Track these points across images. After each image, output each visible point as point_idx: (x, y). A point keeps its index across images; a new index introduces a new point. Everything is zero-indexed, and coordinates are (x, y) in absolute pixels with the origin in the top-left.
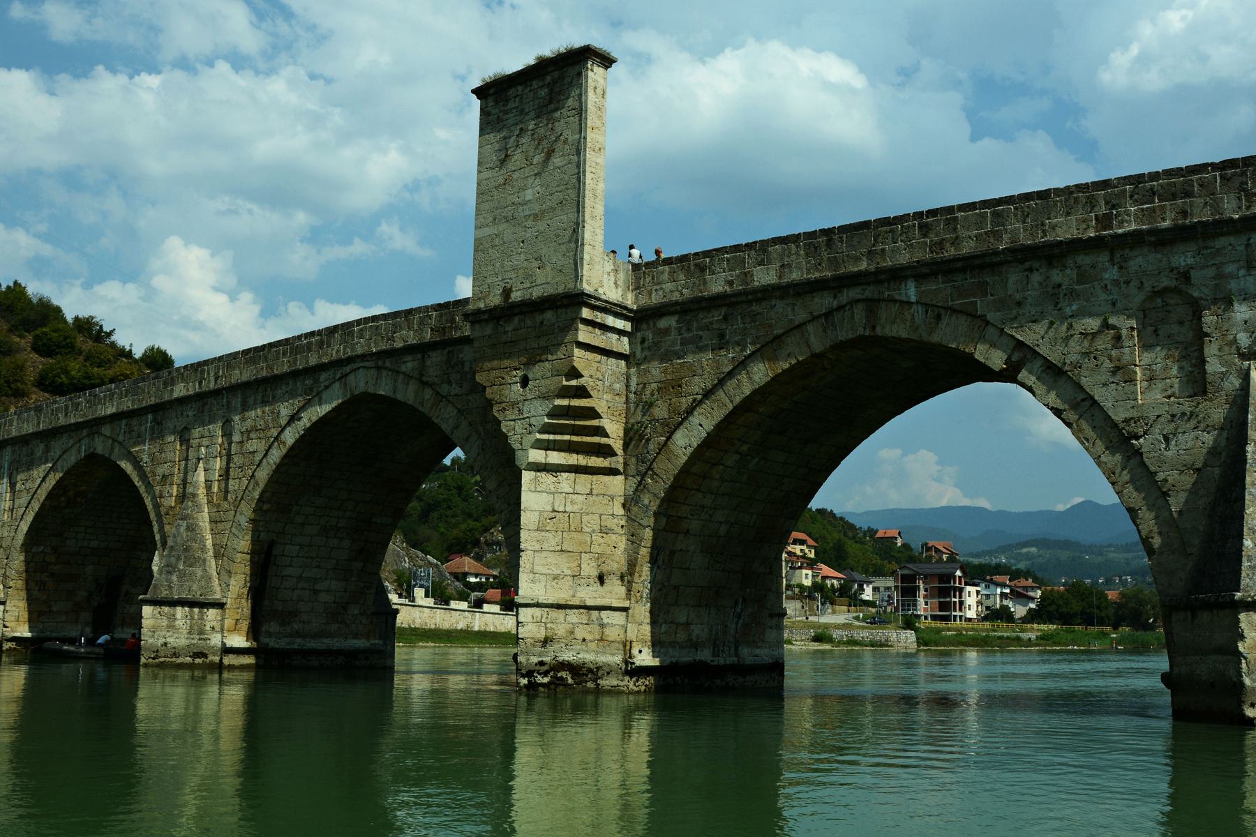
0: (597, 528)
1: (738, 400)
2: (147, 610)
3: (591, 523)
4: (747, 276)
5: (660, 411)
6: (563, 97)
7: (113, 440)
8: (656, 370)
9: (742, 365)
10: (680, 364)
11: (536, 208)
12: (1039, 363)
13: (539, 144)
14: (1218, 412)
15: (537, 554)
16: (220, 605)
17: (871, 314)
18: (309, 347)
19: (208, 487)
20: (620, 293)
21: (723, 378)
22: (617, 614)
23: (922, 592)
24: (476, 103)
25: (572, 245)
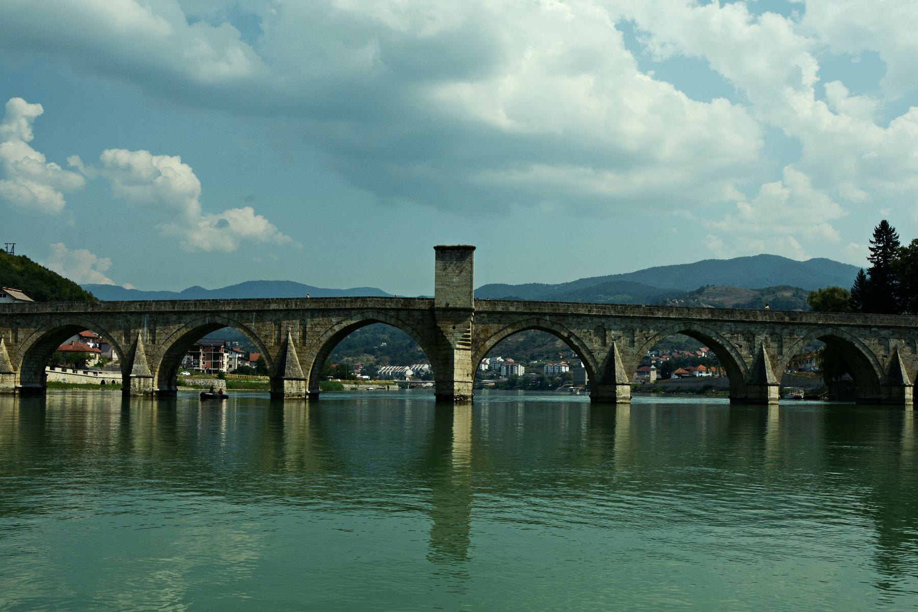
2: (285, 382)
3: (466, 362)
4: (507, 308)
5: (482, 336)
7: (229, 319)
8: (481, 327)
9: (505, 328)
11: (457, 284)
12: (574, 337)
13: (457, 267)
14: (608, 349)
16: (305, 380)
18: (346, 302)
19: (294, 341)
23: (202, 356)
24: (434, 251)
25: (469, 296)
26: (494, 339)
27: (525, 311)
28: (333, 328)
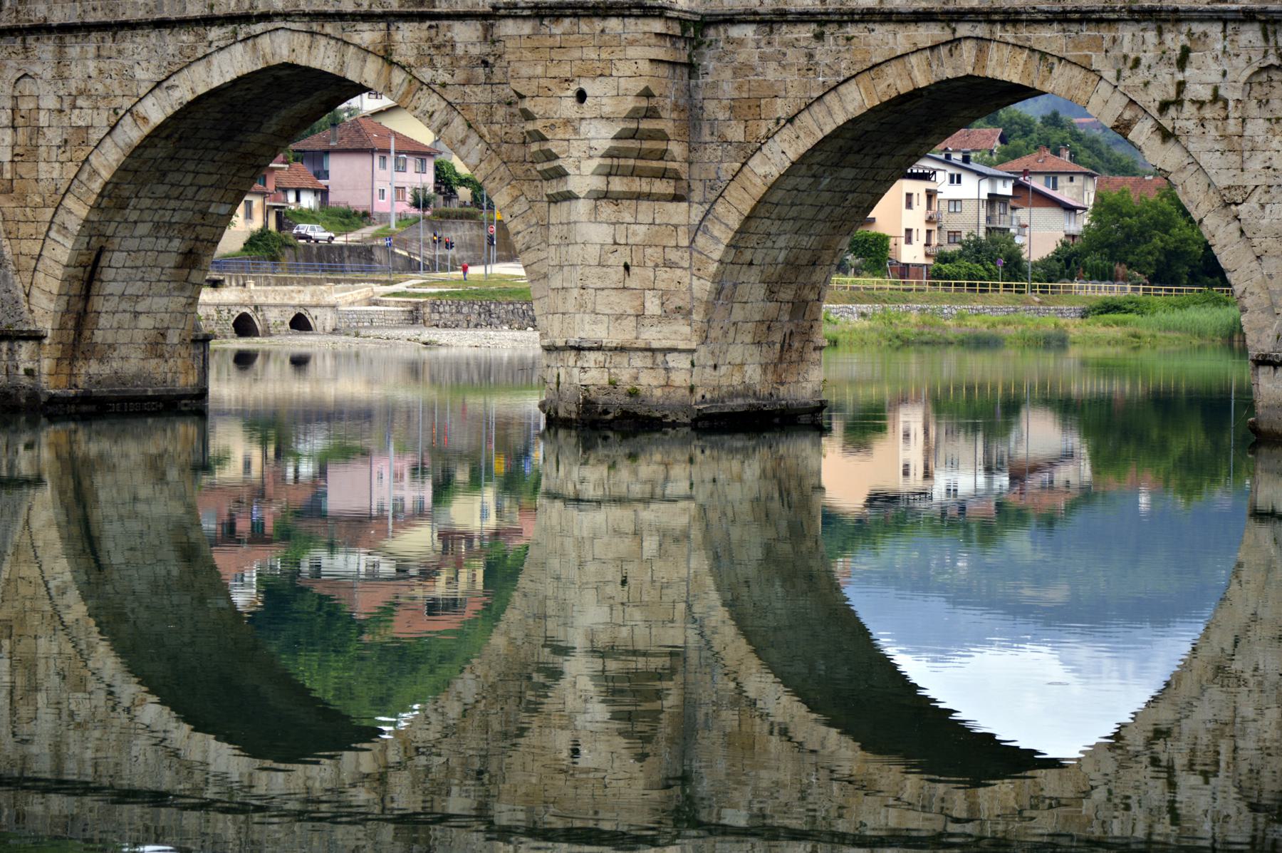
0: (660, 261)
1: (828, 129)
10: (758, 81)
15: (598, 292)
17: (981, 54)
21: (810, 104)
22: (683, 356)
26: (785, 146)
28: (140, 108)
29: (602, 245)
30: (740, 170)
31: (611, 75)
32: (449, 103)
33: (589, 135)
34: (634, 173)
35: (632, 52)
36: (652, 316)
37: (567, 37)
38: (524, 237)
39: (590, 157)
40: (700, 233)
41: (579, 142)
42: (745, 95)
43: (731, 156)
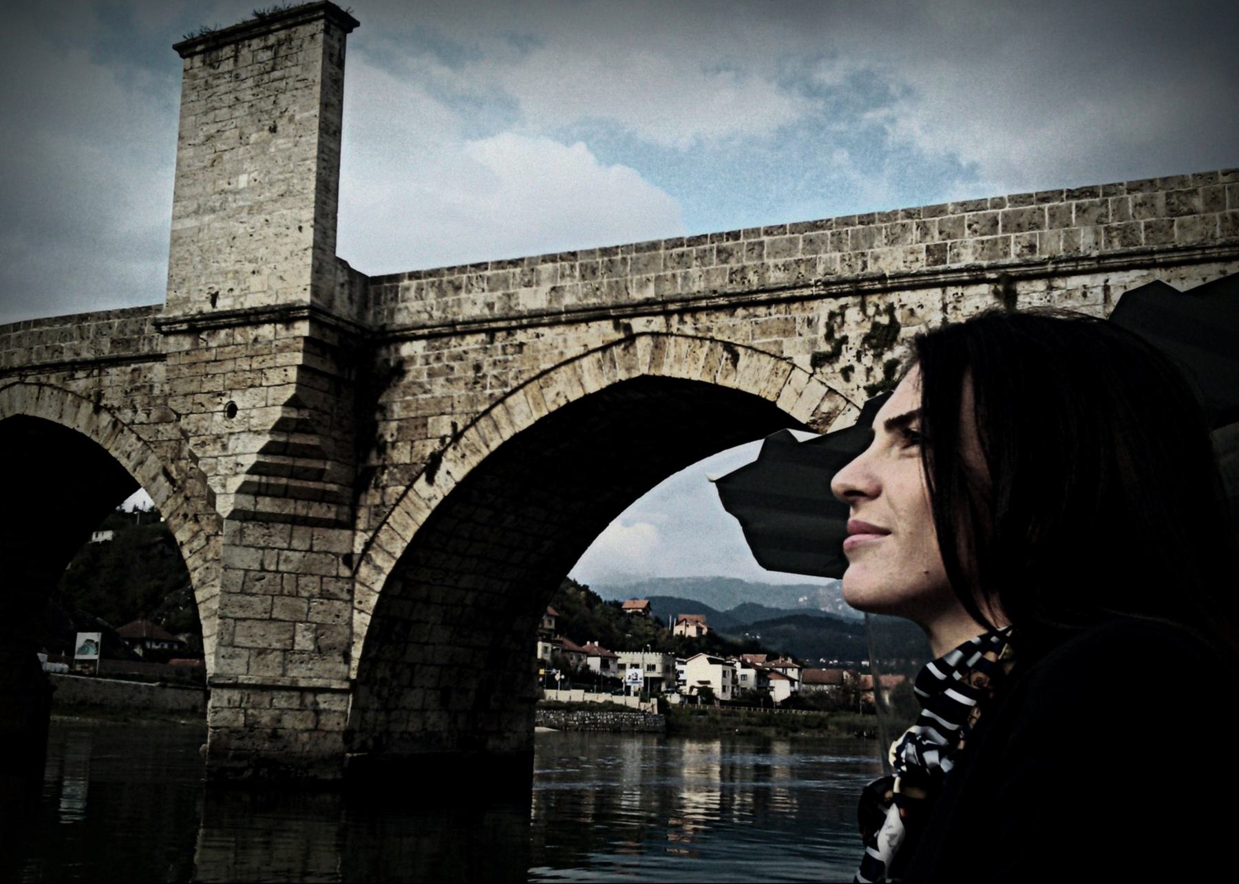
0: (316, 591)
1: (494, 445)
6: (289, 64)
10: (426, 400)
15: (239, 623)
20: (355, 310)
22: (337, 697)
27: (593, 301)
29: (247, 571)
30: (405, 494)
31: (261, 385)
32: (145, 442)
33: (237, 451)
34: (284, 493)
35: (281, 359)
36: (302, 652)
37: (222, 349)
38: (200, 573)
39: (236, 474)
40: (363, 563)
41: (227, 459)
42: (412, 414)
43: (396, 480)
